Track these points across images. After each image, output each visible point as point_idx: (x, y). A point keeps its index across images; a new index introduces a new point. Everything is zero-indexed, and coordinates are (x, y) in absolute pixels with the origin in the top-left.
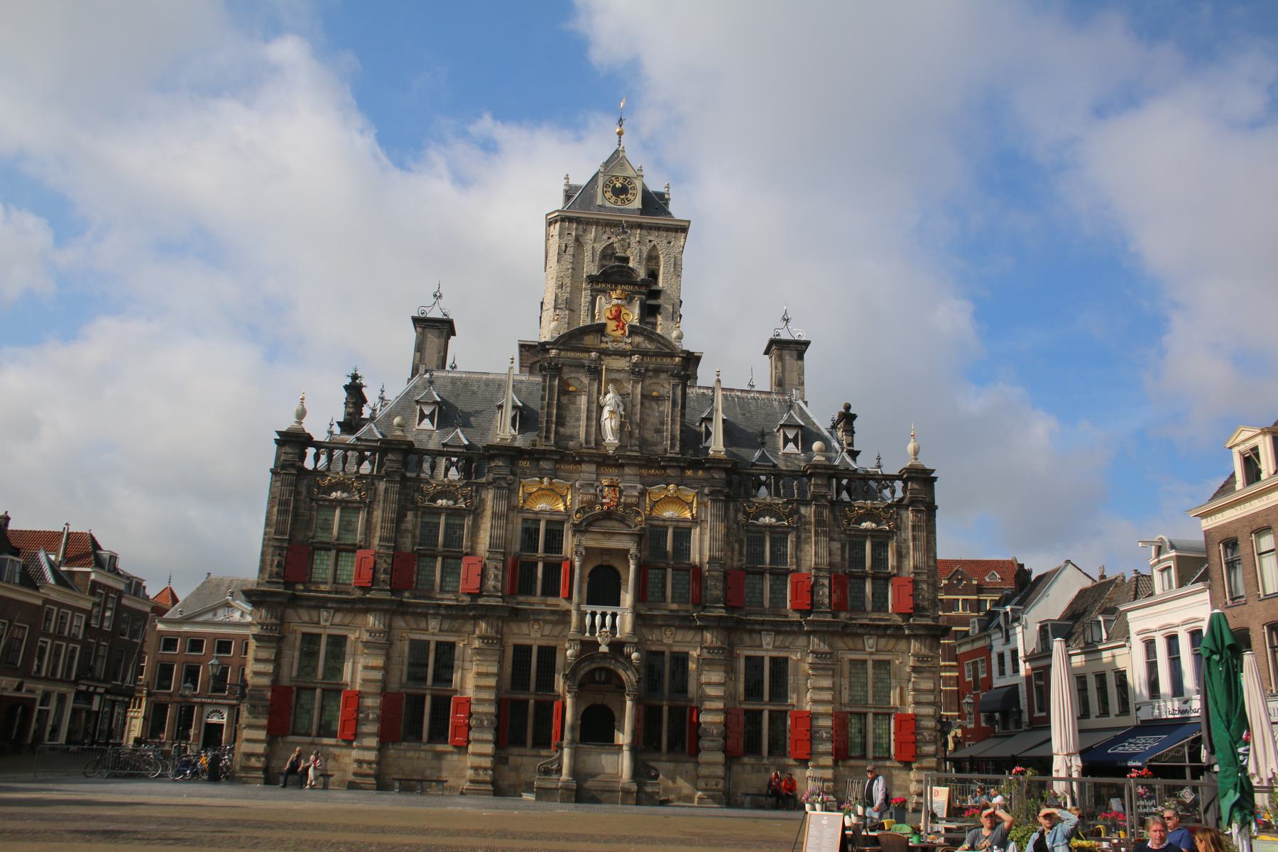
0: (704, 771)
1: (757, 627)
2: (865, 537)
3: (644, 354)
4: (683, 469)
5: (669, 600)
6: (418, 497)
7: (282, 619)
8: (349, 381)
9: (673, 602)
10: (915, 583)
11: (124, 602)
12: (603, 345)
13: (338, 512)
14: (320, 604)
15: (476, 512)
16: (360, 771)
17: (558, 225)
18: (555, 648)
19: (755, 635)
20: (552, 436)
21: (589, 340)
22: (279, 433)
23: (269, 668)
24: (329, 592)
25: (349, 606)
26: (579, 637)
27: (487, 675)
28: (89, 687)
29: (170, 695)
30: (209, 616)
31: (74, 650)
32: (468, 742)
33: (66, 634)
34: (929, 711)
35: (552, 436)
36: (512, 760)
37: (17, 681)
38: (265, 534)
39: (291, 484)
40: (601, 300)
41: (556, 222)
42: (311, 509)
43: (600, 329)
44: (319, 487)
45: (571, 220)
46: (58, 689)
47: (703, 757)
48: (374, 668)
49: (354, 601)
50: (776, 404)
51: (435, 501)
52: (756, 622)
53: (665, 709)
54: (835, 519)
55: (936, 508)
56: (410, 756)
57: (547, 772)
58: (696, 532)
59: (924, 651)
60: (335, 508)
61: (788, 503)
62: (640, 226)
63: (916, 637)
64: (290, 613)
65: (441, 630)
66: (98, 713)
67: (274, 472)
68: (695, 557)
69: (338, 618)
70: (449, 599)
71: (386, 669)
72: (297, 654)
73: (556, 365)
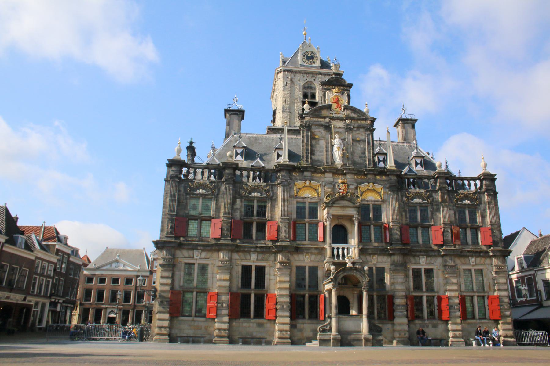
0: (398, 328)
1: (418, 254)
2: (465, 208)
3: (352, 119)
4: (376, 175)
5: (373, 241)
6: (242, 192)
7: (174, 256)
8: (188, 144)
9: (375, 242)
10: (492, 230)
11: (71, 259)
12: (332, 115)
13: (201, 200)
14: (194, 247)
15: (273, 199)
16: (220, 334)
17: (282, 73)
18: (317, 267)
19: (416, 258)
20: (310, 160)
21: (324, 113)
22: (169, 160)
23: (169, 281)
24: (198, 241)
25: (209, 248)
26: (332, 260)
27: (284, 282)
28: (56, 299)
29: (91, 304)
31: (49, 281)
32: (276, 317)
33: (45, 274)
34: (505, 293)
35: (310, 160)
36: (299, 326)
37: (23, 296)
38: (163, 212)
39: (176, 186)
40: (328, 93)
41: (281, 72)
42: (186, 199)
43: (329, 107)
44: (190, 187)
45: (288, 71)
46: (41, 300)
47: (397, 321)
48: (224, 280)
49: (212, 245)
50: (407, 148)
51: (251, 194)
52: (417, 251)
53: (375, 296)
54: (450, 199)
55: (497, 193)
56: (248, 326)
57: (324, 331)
58: (383, 207)
59: (500, 264)
60: (199, 198)
61: (427, 192)
62: (320, 74)
63: (494, 256)
64: (179, 253)
65: (257, 260)
66: (59, 312)
67: (166, 181)
68: (384, 219)
69: (204, 254)
70: (261, 244)
71: (230, 280)
72: (182, 274)
73: (309, 125)
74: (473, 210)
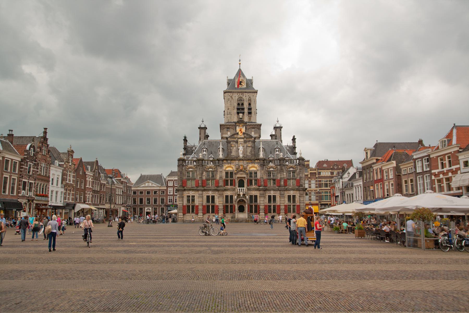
6: (206, 169)
15: (217, 171)
21: (235, 136)
30: (144, 185)
45: (229, 92)
47: (261, 214)
69: (193, 192)
74: (294, 172)
